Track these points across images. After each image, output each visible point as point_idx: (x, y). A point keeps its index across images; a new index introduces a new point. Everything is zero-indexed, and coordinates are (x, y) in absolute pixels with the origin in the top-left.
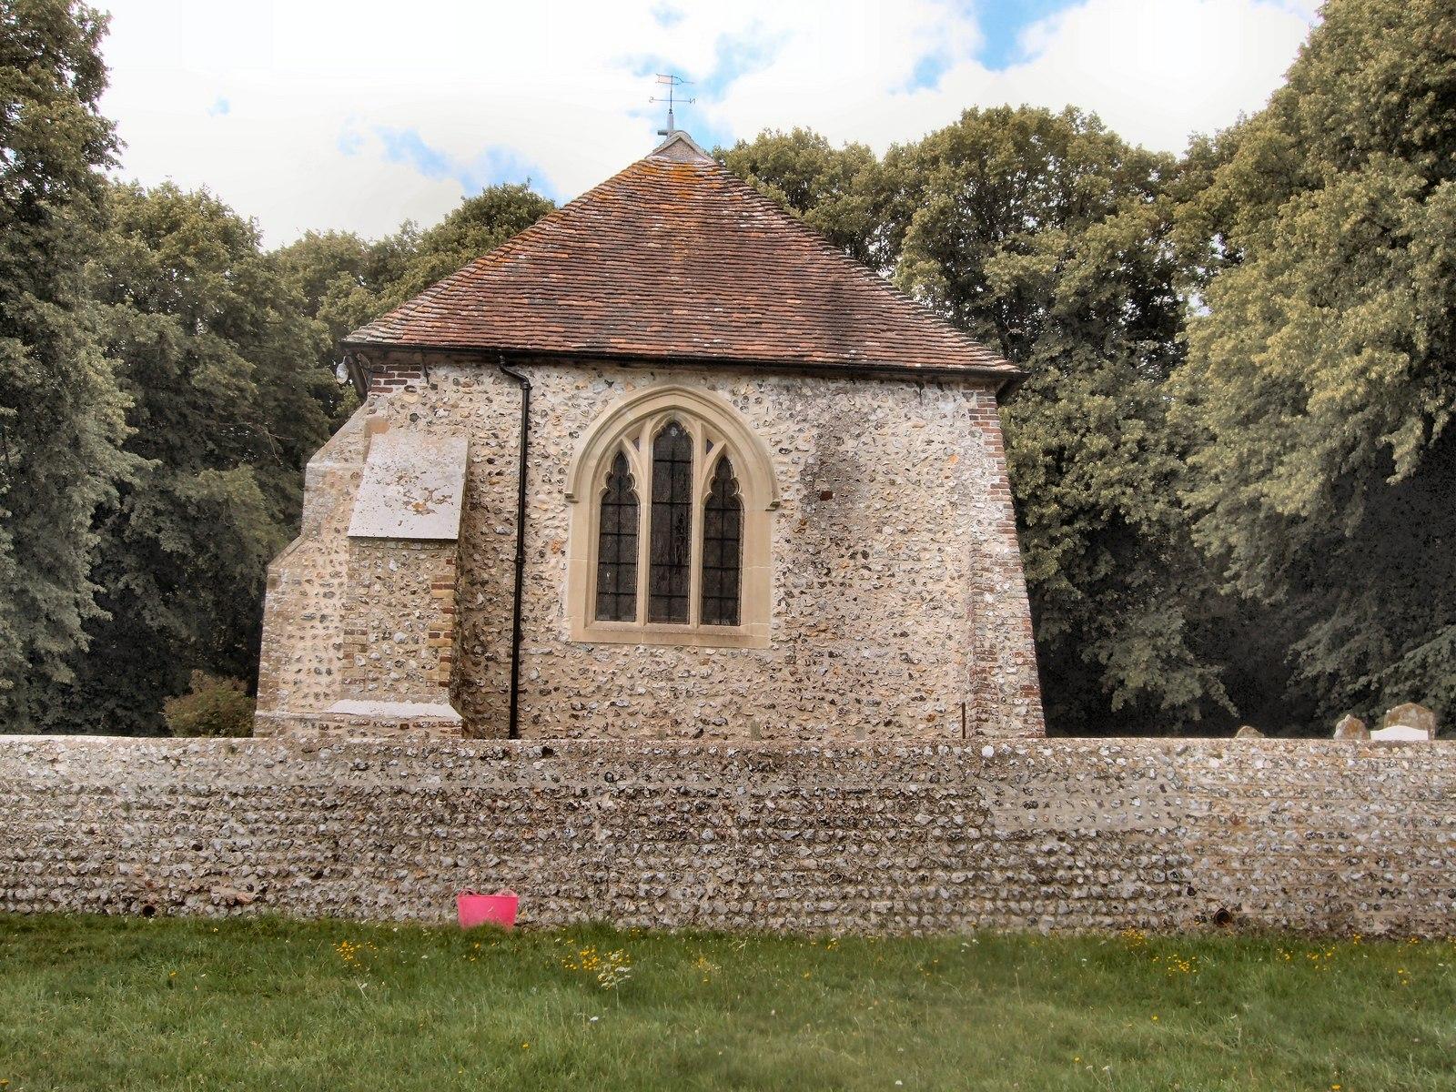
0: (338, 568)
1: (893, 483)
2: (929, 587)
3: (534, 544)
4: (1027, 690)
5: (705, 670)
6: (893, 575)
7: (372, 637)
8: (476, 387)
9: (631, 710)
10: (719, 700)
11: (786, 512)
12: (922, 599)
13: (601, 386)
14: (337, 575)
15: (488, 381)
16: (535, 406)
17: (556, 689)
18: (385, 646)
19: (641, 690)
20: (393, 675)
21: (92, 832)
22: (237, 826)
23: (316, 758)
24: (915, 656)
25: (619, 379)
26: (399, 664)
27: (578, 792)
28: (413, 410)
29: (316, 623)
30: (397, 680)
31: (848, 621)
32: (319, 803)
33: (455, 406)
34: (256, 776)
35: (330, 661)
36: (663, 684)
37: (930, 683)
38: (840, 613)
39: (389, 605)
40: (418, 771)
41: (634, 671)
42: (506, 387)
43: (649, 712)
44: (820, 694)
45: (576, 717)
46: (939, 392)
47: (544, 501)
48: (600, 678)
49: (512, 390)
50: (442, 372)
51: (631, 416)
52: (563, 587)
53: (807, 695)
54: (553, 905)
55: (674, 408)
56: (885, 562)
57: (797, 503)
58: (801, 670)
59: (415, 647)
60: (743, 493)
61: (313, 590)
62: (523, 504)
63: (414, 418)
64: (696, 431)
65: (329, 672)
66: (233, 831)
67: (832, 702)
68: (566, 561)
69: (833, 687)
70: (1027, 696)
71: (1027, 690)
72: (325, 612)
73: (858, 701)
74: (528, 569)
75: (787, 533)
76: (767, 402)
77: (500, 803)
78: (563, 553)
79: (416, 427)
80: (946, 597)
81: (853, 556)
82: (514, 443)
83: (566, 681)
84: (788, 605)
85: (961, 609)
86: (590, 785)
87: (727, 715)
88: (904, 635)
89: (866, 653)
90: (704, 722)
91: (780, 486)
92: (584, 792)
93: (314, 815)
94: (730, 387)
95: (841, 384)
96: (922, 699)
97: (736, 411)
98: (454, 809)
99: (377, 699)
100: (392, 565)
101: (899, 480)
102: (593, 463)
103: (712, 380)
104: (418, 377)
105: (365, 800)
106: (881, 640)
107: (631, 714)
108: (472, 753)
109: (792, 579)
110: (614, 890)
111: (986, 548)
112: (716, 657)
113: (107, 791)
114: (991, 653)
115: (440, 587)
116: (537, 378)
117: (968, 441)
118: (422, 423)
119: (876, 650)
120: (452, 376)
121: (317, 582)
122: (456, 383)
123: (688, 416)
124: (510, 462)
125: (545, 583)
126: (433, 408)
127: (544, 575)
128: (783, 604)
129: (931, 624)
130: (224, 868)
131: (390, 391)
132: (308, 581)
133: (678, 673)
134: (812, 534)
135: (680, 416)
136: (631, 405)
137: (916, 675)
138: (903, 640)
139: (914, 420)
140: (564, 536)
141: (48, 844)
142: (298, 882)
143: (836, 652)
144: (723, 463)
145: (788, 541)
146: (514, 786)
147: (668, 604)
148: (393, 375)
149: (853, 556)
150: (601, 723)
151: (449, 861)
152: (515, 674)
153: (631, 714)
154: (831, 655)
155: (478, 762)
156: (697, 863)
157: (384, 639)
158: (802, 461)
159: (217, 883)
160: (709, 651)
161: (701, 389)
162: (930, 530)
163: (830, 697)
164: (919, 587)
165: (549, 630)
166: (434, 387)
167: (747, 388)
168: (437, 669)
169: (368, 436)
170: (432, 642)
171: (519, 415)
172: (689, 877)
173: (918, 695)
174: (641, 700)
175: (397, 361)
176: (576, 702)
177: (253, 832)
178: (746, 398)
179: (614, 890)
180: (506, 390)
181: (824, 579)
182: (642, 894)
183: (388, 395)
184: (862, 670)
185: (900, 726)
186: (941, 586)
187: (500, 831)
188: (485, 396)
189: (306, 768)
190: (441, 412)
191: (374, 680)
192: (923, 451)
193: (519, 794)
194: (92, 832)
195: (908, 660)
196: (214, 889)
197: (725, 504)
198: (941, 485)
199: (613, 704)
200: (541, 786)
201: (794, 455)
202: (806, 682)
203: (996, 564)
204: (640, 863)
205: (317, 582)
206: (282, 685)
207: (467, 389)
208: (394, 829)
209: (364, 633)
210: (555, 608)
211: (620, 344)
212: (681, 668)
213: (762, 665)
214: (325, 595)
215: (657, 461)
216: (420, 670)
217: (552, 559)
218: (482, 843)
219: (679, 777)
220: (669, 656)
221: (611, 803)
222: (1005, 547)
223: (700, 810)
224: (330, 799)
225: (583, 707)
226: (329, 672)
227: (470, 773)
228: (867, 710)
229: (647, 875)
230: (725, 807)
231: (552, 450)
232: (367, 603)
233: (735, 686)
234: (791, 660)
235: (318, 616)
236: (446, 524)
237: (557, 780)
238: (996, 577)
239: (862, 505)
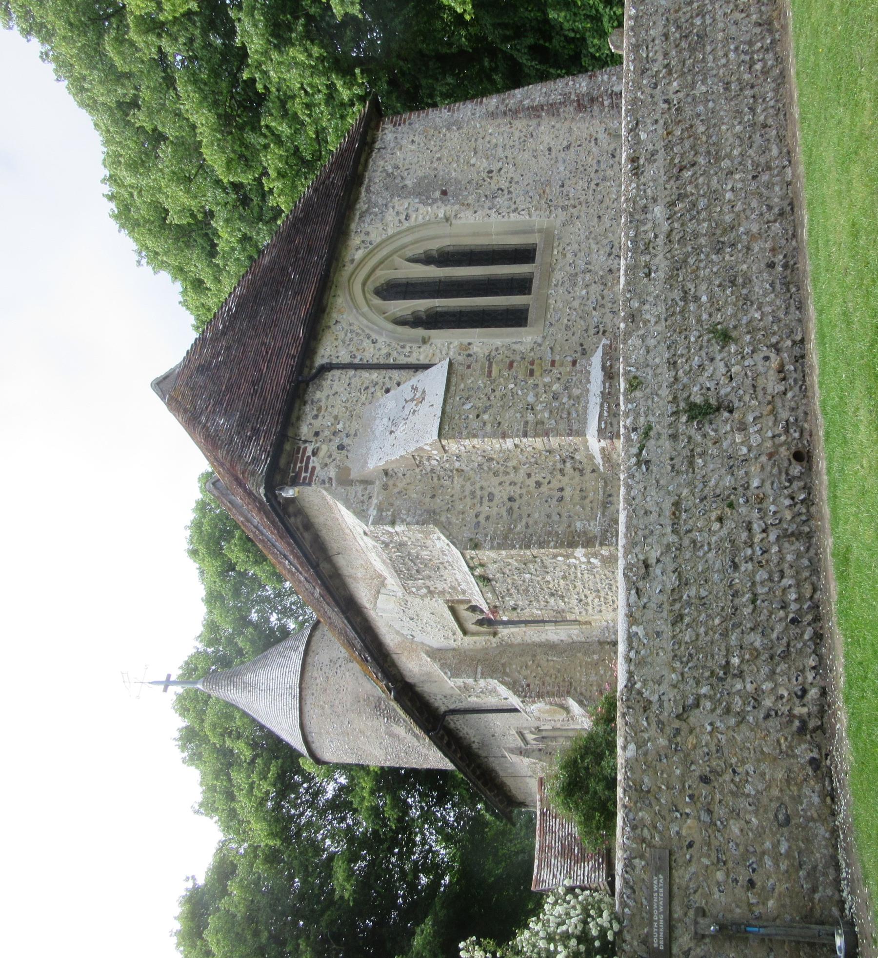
0: (467, 493)
1: (439, 159)
2: (516, 139)
5: (569, 255)
6: (506, 157)
7: (530, 417)
8: (323, 404)
9: (600, 298)
10: (594, 247)
11: (453, 214)
12: (525, 141)
13: (339, 327)
14: (473, 493)
15: (318, 395)
17: (582, 345)
18: (539, 407)
19: (584, 292)
20: (565, 400)
21: (720, 519)
22: (706, 374)
23: (639, 310)
24: (565, 143)
25: (335, 315)
26: (555, 397)
27: (666, 106)
28: (334, 448)
29: (516, 505)
30: (570, 397)
31: (537, 179)
32: (682, 304)
33: (336, 417)
34: (657, 360)
35: (550, 489)
36: (579, 279)
37: (585, 136)
38: (531, 182)
39: (503, 407)
40: (649, 225)
41: (569, 297)
42: (326, 384)
43: (602, 287)
44: (591, 192)
45: (604, 332)
48: (573, 317)
49: (330, 378)
50: (305, 430)
51: (365, 309)
52: (498, 342)
53: (591, 198)
54: (762, 118)
55: (364, 284)
56: (496, 161)
57: (448, 207)
58: (572, 202)
59: (541, 385)
61: (485, 509)
63: (341, 447)
64: (384, 275)
65: (561, 489)
66: (711, 378)
67: (597, 185)
69: (586, 184)
70: (595, 76)
72: (506, 498)
73: (597, 171)
75: (469, 213)
76: (370, 229)
77: (676, 161)
78: (470, 344)
79: (349, 445)
80: (524, 130)
81: (491, 178)
82: (374, 375)
83: (575, 339)
84: (523, 210)
85: (533, 123)
86: (659, 99)
87: (605, 242)
88: (550, 149)
90: (610, 255)
91: (433, 220)
92: (666, 101)
93: (692, 307)
94: (353, 251)
95: (363, 190)
96: (596, 139)
97: (371, 247)
98: (681, 197)
99: (586, 408)
100: (467, 407)
101: (438, 155)
103: (347, 259)
104: (305, 449)
105: (677, 266)
106: (552, 162)
107: (603, 298)
108: (634, 185)
109: (504, 211)
110: (747, 76)
112: (560, 248)
113: (677, 504)
115: (490, 372)
118: (346, 441)
120: (309, 418)
121: (478, 508)
122: (316, 417)
123: (372, 279)
124: (390, 378)
125: (493, 354)
126: (335, 433)
127: (487, 354)
128: (523, 213)
129: (543, 137)
130: (749, 382)
131: (314, 468)
132: (477, 516)
133: (571, 270)
134: (471, 199)
135: (370, 286)
137: (579, 143)
138: (553, 150)
140: (456, 343)
141: (735, 566)
142: (757, 315)
143: (560, 183)
145: (475, 212)
146: (662, 152)
148: (300, 468)
150: (610, 316)
151: (729, 195)
153: (603, 298)
154: (563, 186)
155: (643, 180)
156: (721, 25)
157: (532, 409)
158: (417, 205)
159: (764, 389)
160: (555, 252)
161: (349, 268)
162: (476, 140)
163: (593, 186)
164: (517, 143)
165: (532, 349)
166: (317, 434)
167: (355, 240)
168: (561, 369)
169: (351, 483)
170: (537, 374)
171: (352, 372)
172: (733, 30)
173: (593, 142)
174: (592, 292)
175: (289, 463)
176: (592, 331)
177: (712, 360)
178: (363, 242)
179: (747, 76)
180: (329, 382)
181: (506, 192)
182: (747, 58)
183: (318, 469)
184: (574, 170)
185: (615, 149)
186: (517, 134)
187: (702, 160)
188: (331, 397)
189: (648, 317)
190: (340, 427)
191: (569, 414)
192: (419, 144)
193: (668, 147)
194: (720, 519)
195: (568, 147)
196: (769, 391)
197: (445, 258)
198: (445, 135)
199: (595, 309)
200: (661, 131)
201: (410, 212)
202: (581, 200)
204: (723, 61)
205: (478, 508)
206: (572, 528)
207: (323, 408)
208: (703, 241)
209: (527, 423)
210: (514, 347)
212: (568, 268)
214: (490, 500)
215: (404, 299)
216: (562, 380)
218: (712, 172)
219: (653, 40)
220: (558, 276)
221: (675, 84)
222: (493, 102)
223: (679, 27)
224: (677, 294)
225: (597, 327)
226: (561, 489)
227: (651, 184)
228: (603, 166)
229: (732, 55)
230: (677, 11)
231: (384, 351)
232: (499, 423)
233: (583, 237)
234: (564, 208)
235: (509, 504)
237: (656, 121)
239: (454, 174)
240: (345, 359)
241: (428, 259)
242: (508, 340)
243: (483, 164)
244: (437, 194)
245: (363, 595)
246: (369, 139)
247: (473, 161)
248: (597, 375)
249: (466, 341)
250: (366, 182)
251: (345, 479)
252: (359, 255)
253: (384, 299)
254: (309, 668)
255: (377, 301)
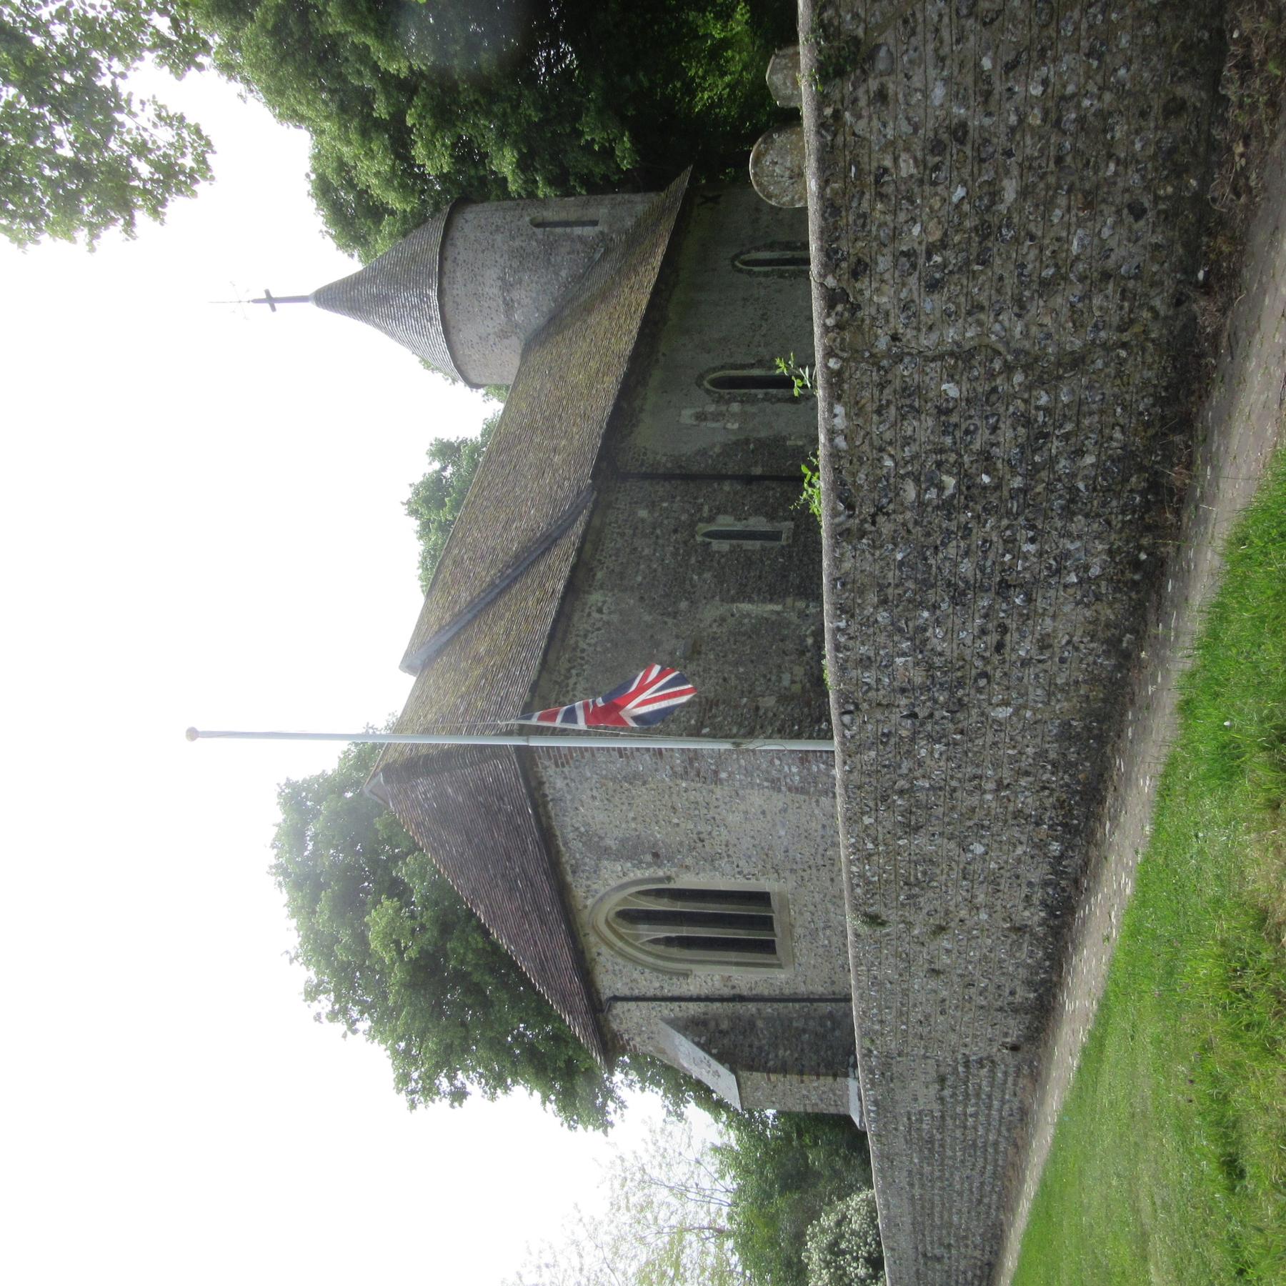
1: (634, 819)
3: (727, 992)
13: (602, 959)
16: (627, 992)
25: (594, 950)
46: (547, 785)
47: (692, 987)
51: (620, 944)
68: (735, 975)
74: (745, 993)
89: (782, 833)
97: (598, 896)
102: (660, 963)
111: (679, 770)
114: (773, 781)
116: (606, 993)
119: (778, 827)
136: (610, 945)
139: (577, 804)
149: (702, 841)
164: (720, 803)
167: (579, 892)
195: (785, 810)
203: (692, 766)
234: (792, 871)
241: (659, 893)
242: (765, 976)
244: (649, 858)
246: (533, 784)
247: (676, 821)
249: (727, 975)
250: (558, 833)
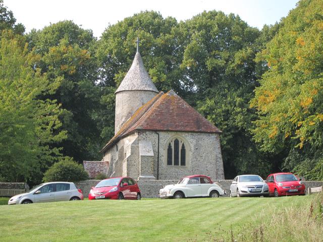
3: (160, 155)
4: (222, 174)
50: (147, 133)
60: (186, 148)
62: (158, 150)
71: (222, 174)
82: (157, 142)
105: (153, 187)
117: (215, 142)
144: (183, 145)
147: (176, 163)
152: (158, 172)
167: (187, 134)
211: (170, 129)
213: (189, 171)
217: (162, 157)
220: (177, 170)
222: (220, 156)
236: (152, 154)
238: (219, 159)
240: (160, 137)
241: (183, 146)
243: (204, 155)
245: (129, 137)
248: (150, 177)
251: (139, 140)
252: (183, 135)
253: (175, 141)
254: (140, 92)
255: (174, 140)
